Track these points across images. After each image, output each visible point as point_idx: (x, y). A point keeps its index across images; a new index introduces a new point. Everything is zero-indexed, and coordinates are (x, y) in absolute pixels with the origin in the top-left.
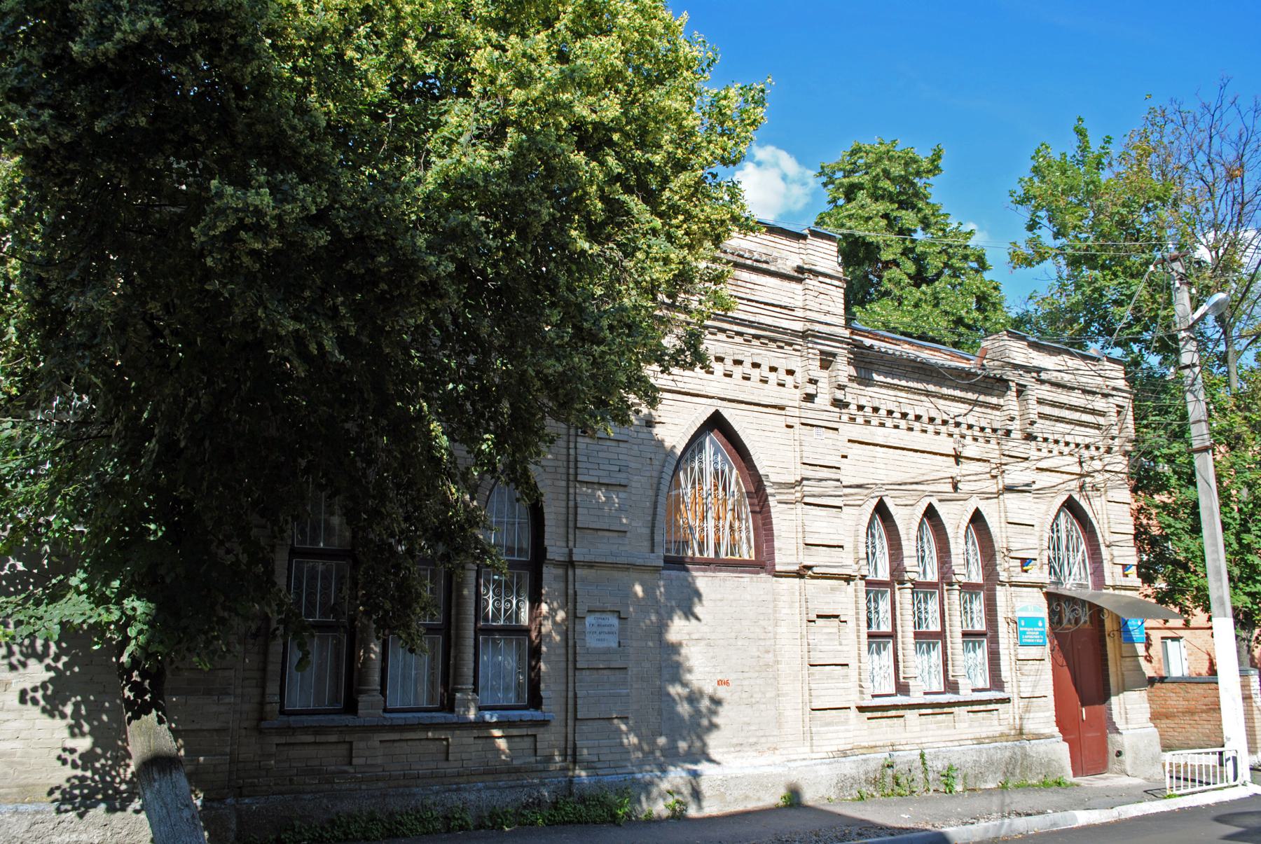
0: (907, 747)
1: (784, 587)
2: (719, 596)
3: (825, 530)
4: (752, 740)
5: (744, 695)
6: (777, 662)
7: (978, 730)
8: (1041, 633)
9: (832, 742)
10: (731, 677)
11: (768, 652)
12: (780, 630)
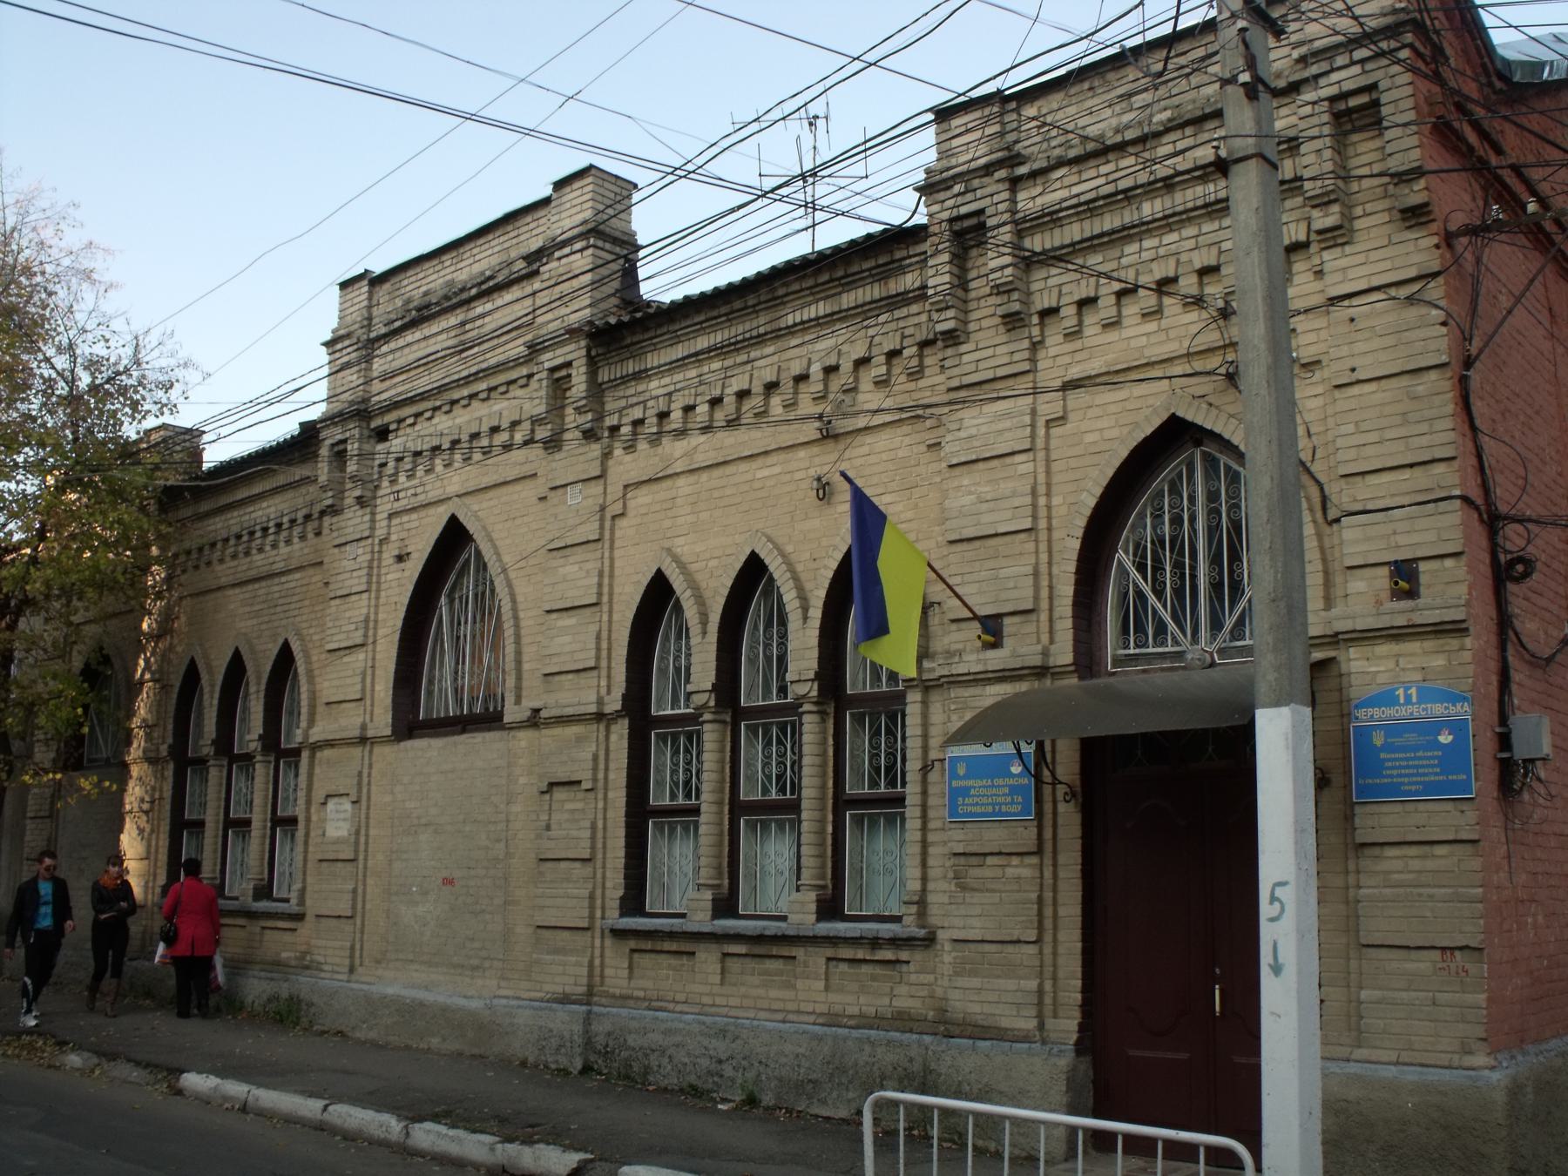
0: (679, 1008)
3: (567, 649)
4: (475, 962)
7: (850, 999)
8: (1014, 790)
9: (558, 979)
11: (498, 841)
12: (516, 808)
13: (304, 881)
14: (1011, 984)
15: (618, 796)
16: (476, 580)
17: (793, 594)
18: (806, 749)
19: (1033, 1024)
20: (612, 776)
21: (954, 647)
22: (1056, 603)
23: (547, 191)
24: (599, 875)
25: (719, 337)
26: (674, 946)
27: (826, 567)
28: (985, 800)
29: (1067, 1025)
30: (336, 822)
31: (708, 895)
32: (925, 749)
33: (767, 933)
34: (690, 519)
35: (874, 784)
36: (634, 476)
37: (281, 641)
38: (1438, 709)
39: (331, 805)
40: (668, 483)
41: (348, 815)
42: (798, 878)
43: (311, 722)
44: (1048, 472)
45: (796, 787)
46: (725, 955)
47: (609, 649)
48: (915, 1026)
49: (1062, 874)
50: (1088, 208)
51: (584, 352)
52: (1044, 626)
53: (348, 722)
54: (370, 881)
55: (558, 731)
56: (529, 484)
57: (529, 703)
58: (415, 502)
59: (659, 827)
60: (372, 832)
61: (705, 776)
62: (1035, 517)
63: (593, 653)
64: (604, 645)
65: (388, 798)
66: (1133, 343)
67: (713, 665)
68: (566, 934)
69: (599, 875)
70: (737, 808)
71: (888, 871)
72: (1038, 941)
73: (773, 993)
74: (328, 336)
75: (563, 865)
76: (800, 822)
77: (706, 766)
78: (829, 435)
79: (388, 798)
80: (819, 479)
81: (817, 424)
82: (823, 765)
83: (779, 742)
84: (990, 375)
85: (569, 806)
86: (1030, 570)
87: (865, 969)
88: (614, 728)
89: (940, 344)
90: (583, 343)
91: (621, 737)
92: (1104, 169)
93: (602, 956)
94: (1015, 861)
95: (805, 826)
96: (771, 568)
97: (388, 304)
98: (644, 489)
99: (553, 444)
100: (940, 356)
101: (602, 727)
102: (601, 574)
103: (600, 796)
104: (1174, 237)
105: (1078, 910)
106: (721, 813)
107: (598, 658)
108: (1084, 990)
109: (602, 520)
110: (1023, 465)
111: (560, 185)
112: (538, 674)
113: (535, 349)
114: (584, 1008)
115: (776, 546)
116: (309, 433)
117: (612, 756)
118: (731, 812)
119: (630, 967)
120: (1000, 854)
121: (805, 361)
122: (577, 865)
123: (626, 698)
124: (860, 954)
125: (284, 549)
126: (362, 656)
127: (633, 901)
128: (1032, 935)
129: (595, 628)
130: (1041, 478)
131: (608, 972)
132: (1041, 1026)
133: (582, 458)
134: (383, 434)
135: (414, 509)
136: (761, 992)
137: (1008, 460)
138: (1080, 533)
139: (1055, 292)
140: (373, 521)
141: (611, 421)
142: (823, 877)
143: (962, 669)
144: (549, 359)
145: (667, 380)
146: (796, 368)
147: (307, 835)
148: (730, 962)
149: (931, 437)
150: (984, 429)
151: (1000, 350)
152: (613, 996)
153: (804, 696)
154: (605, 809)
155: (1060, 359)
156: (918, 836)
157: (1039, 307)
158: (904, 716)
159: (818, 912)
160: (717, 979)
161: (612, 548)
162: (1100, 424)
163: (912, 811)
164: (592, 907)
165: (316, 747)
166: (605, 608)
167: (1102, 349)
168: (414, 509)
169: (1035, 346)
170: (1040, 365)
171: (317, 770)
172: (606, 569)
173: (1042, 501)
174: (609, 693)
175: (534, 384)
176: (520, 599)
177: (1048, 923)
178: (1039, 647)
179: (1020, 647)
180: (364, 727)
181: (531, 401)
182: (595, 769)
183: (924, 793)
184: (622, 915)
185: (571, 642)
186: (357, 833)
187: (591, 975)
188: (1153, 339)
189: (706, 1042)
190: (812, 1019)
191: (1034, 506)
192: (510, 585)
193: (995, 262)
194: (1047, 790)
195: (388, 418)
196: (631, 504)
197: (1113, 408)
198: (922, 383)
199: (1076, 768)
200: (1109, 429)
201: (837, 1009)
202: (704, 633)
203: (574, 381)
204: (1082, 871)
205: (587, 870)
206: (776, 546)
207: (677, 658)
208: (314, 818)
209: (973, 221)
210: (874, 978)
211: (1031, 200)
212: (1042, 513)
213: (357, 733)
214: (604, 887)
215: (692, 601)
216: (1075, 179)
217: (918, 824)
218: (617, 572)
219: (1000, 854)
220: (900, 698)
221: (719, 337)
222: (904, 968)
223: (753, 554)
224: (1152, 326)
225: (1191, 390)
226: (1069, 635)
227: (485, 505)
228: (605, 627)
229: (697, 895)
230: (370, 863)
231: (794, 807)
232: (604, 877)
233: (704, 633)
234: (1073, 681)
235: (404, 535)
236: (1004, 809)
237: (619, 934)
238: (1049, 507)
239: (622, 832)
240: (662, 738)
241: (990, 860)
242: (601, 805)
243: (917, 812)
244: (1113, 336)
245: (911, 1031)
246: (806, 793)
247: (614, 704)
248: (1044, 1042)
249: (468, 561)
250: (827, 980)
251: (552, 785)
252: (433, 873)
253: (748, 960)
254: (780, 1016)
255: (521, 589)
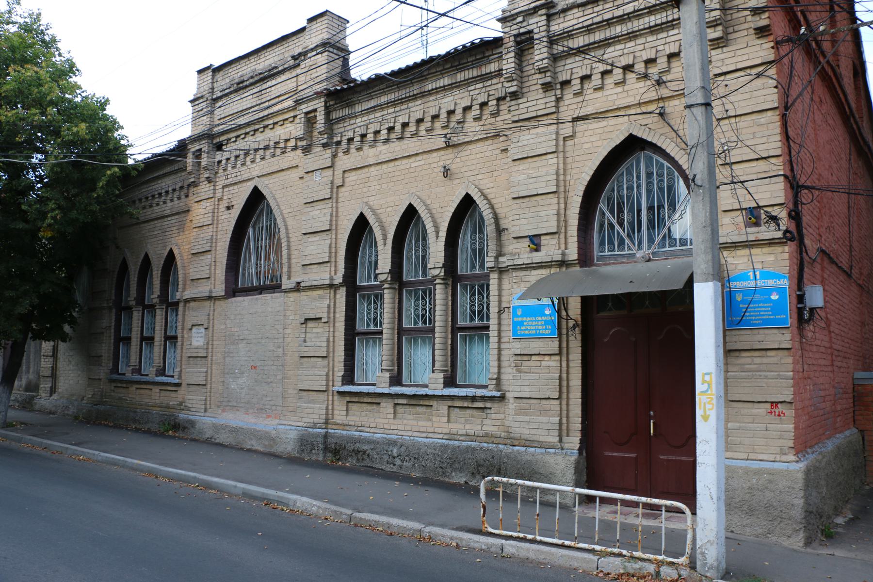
1: (292, 300)
2: (254, 311)
3: (315, 252)
5: (265, 376)
6: (284, 354)
7: (461, 426)
9: (310, 416)
10: (258, 364)
12: (288, 331)
13: (181, 367)
14: (544, 419)
15: (341, 326)
16: (267, 219)
17: (431, 224)
18: (437, 302)
19: (557, 439)
20: (337, 315)
21: (514, 251)
22: (569, 229)
23: (304, 23)
24: (331, 364)
25: (393, 96)
26: (369, 400)
27: (448, 211)
28: (531, 328)
29: (574, 441)
30: (197, 339)
31: (387, 374)
32: (500, 302)
33: (418, 393)
34: (378, 187)
35: (472, 319)
36: (348, 166)
37: (168, 249)
38: (771, 282)
39: (194, 330)
40: (366, 170)
41: (203, 335)
42: (433, 366)
43: (184, 289)
44: (565, 163)
45: (432, 321)
46: (396, 404)
47: (336, 253)
48: (495, 440)
49: (571, 365)
50: (589, 29)
51: (323, 104)
52: (563, 241)
53: (203, 290)
54: (214, 367)
55: (309, 293)
56: (294, 170)
57: (295, 279)
58: (236, 180)
59: (361, 341)
60: (215, 343)
61: (385, 315)
62: (557, 186)
63: (327, 254)
64: (333, 250)
65: (223, 326)
66: (610, 98)
67: (390, 260)
68: (314, 393)
69: (331, 364)
70: (401, 331)
71: (481, 363)
72: (560, 398)
73: (420, 423)
74: (192, 98)
75: (312, 359)
76: (434, 338)
77: (385, 311)
78: (448, 146)
79: (223, 326)
80: (445, 167)
81: (444, 139)
82: (446, 310)
83: (423, 299)
84: (534, 114)
85: (315, 330)
86: (555, 212)
87: (468, 412)
88: (338, 292)
89: (508, 99)
90: (322, 100)
91: (342, 296)
92: (596, 9)
93: (333, 404)
94: (547, 358)
95: (437, 341)
96: (420, 212)
97: (224, 81)
98: (354, 173)
99: (307, 150)
100: (508, 105)
101: (332, 291)
102: (331, 215)
103: (332, 325)
104: (632, 44)
105: (579, 383)
106: (393, 334)
107: (330, 257)
108: (583, 423)
109: (332, 188)
110: (552, 160)
111: (311, 20)
112: (299, 265)
113: (298, 103)
114: (325, 430)
115: (422, 201)
116: (182, 147)
117: (337, 305)
118: (398, 333)
119: (347, 410)
120: (539, 354)
121: (437, 108)
122: (320, 359)
123: (344, 277)
124: (466, 405)
125: (169, 204)
126: (209, 256)
127: (349, 377)
128: (556, 395)
129: (329, 241)
130: (561, 166)
131: (336, 412)
132: (561, 441)
133: (322, 157)
134: (219, 147)
135: (235, 184)
136: (415, 422)
137: (544, 157)
138: (581, 193)
139: (569, 72)
140: (215, 189)
141: (335, 139)
142: (446, 366)
143: (520, 262)
144: (305, 108)
145: (365, 118)
146: (433, 111)
147: (182, 344)
148: (399, 408)
149: (503, 146)
150: (531, 141)
151: (539, 102)
152: (338, 424)
153: (437, 276)
154: (334, 332)
155: (571, 106)
156: (496, 345)
157: (560, 80)
158: (488, 286)
159: (444, 383)
160: (392, 416)
161: (337, 202)
162: (592, 139)
163: (493, 333)
164: (327, 380)
165: (187, 301)
166: (334, 232)
167: (594, 102)
168: (235, 184)
169: (558, 100)
170: (561, 109)
171: (187, 313)
172: (334, 213)
173: (562, 177)
174: (335, 274)
175: (297, 120)
176: (290, 227)
177: (564, 389)
178: (560, 251)
179: (550, 250)
180: (211, 292)
181: (296, 129)
182: (329, 312)
183: (499, 324)
184: (343, 384)
185: (318, 248)
186: (208, 343)
187: (327, 414)
188: (620, 96)
189: (386, 448)
190: (441, 436)
191: (557, 180)
192: (284, 221)
193: (540, 54)
194: (564, 322)
195: (222, 138)
196: (347, 180)
197: (599, 131)
198: (498, 119)
199: (579, 311)
200: (595, 144)
201: (454, 431)
202: (385, 244)
203: (318, 118)
204: (582, 363)
205: (325, 362)
206: (422, 201)
207: (370, 257)
208: (186, 336)
209: (528, 36)
210: (473, 416)
211: (557, 26)
212: (562, 183)
213: (207, 294)
214: (333, 371)
215: (379, 228)
216: (581, 14)
217: (496, 339)
218: (340, 214)
219: (539, 354)
220: (487, 276)
221: (393, 96)
222: (489, 411)
223: (410, 204)
224: (620, 89)
225: (640, 122)
226: (576, 245)
227: (271, 181)
228: (334, 241)
229: (380, 374)
230: (214, 358)
231: (432, 330)
232: (333, 366)
233: (385, 244)
234: (578, 268)
235: (230, 196)
236: (542, 332)
237: (340, 393)
238: (565, 181)
239: (343, 343)
240: (363, 297)
241: (534, 358)
242: (332, 330)
243: (496, 333)
244: (599, 94)
245: (493, 443)
246: (437, 324)
247: (338, 279)
248: (562, 449)
249: (262, 210)
250: (448, 417)
251: (306, 320)
252: (257, 365)
253: (407, 407)
254: (424, 435)
255: (291, 223)
